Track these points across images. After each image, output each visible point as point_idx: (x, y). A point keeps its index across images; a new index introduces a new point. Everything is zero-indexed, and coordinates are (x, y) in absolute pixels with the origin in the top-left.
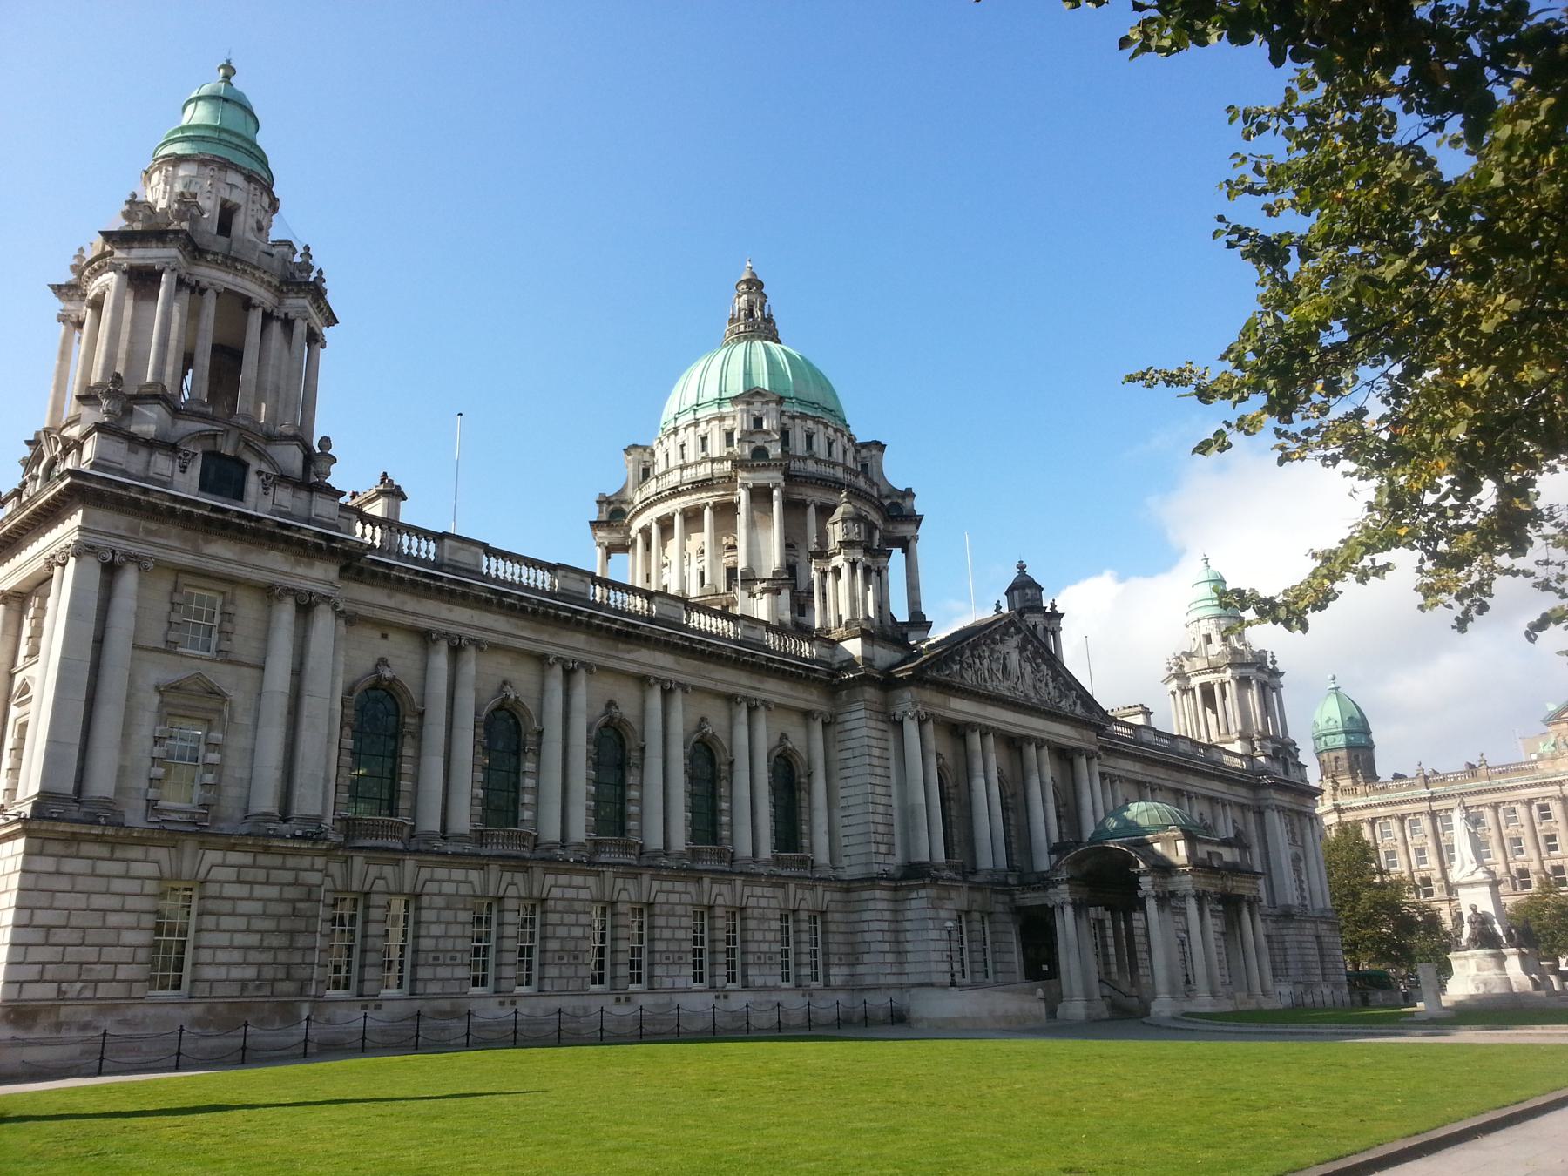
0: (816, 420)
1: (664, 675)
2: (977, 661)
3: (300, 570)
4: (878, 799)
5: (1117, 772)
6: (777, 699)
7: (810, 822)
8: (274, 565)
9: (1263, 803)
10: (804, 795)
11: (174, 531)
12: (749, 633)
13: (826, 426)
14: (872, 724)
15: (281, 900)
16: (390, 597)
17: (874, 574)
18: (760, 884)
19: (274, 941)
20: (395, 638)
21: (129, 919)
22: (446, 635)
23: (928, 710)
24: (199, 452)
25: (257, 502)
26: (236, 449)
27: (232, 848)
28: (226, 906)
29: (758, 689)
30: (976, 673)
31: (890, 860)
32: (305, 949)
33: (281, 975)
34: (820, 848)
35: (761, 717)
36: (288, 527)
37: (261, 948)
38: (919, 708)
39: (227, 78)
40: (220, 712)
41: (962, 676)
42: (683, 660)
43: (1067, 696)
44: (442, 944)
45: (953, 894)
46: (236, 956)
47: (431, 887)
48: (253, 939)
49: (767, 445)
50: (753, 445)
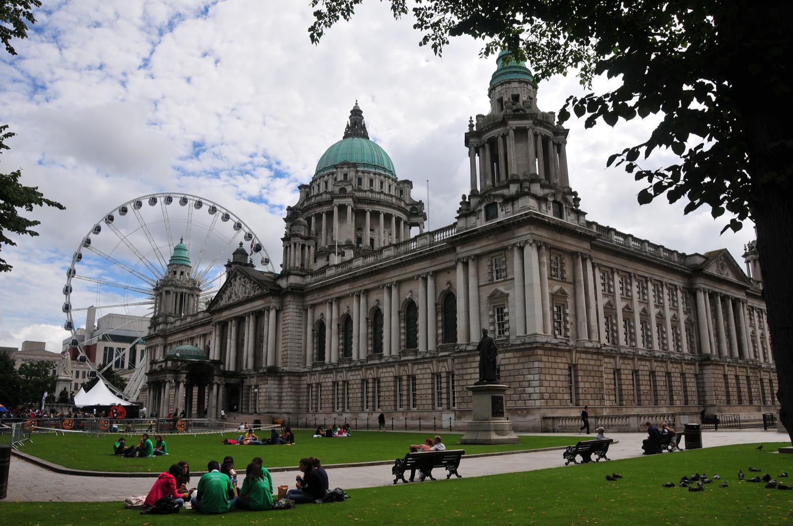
1: (199, 333)
5: (333, 296)
39: (181, 243)
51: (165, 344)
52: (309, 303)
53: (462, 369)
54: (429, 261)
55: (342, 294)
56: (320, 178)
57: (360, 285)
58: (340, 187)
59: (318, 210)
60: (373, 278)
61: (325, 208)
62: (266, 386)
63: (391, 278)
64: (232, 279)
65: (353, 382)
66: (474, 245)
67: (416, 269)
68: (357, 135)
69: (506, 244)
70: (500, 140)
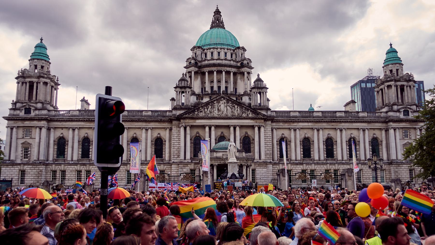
0: (213, 48)
2: (206, 110)
3: (39, 123)
4: (175, 146)
6: (154, 127)
7: (165, 151)
8: (35, 123)
9: (389, 127)
10: (164, 146)
11: (20, 121)
12: (146, 114)
13: (217, 49)
14: (176, 129)
15: (37, 172)
16: (60, 123)
17: (185, 93)
18: (144, 165)
19: (36, 178)
20: (64, 129)
21: (15, 175)
22: (71, 128)
23: (187, 124)
24: (24, 109)
25: (33, 114)
26: (29, 107)
27: (29, 165)
28: (28, 173)
29: (148, 125)
30: (205, 113)
31: (179, 158)
32: (40, 179)
33: (37, 182)
34: (166, 156)
35: (149, 131)
36: (34, 117)
37: (34, 179)
38: (183, 124)
39: (41, 42)
40: (30, 146)
41: (199, 114)
42: (126, 123)
43: (246, 113)
44: (70, 178)
45: (189, 165)
46: (30, 180)
47: (67, 169)
48: (33, 177)
49: (191, 61)
50: (189, 62)
51: (49, 127)
52: (274, 127)
53: (397, 169)
54: (367, 124)
55: (304, 127)
56: (221, 49)
57: (321, 125)
58: (247, 62)
59: (228, 69)
60: (329, 123)
61: (234, 70)
62: (264, 170)
63: (343, 126)
64: (215, 101)
65: (319, 170)
66: (399, 124)
67: (359, 125)
68: (218, 27)
69: (414, 127)
70: (405, 87)
